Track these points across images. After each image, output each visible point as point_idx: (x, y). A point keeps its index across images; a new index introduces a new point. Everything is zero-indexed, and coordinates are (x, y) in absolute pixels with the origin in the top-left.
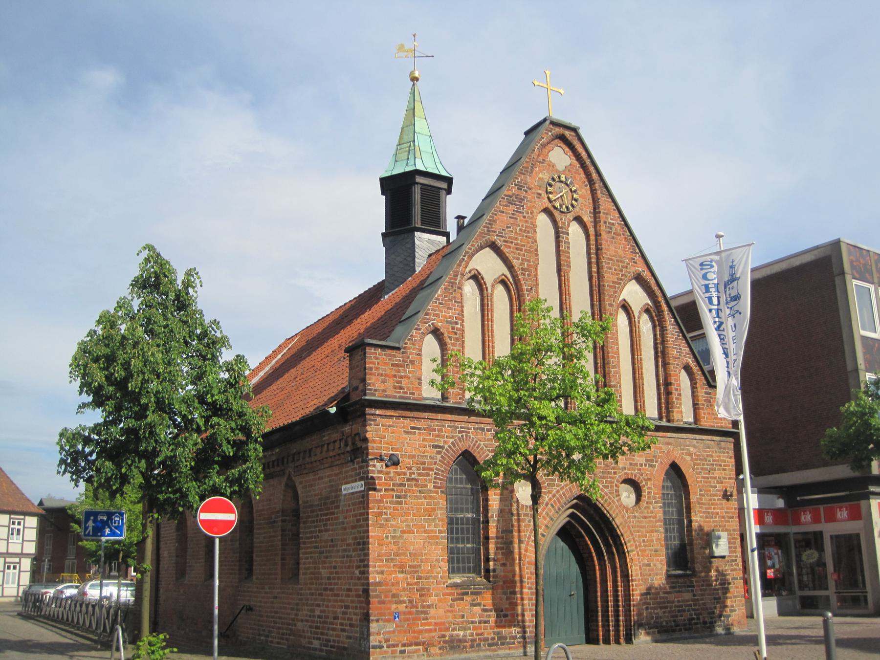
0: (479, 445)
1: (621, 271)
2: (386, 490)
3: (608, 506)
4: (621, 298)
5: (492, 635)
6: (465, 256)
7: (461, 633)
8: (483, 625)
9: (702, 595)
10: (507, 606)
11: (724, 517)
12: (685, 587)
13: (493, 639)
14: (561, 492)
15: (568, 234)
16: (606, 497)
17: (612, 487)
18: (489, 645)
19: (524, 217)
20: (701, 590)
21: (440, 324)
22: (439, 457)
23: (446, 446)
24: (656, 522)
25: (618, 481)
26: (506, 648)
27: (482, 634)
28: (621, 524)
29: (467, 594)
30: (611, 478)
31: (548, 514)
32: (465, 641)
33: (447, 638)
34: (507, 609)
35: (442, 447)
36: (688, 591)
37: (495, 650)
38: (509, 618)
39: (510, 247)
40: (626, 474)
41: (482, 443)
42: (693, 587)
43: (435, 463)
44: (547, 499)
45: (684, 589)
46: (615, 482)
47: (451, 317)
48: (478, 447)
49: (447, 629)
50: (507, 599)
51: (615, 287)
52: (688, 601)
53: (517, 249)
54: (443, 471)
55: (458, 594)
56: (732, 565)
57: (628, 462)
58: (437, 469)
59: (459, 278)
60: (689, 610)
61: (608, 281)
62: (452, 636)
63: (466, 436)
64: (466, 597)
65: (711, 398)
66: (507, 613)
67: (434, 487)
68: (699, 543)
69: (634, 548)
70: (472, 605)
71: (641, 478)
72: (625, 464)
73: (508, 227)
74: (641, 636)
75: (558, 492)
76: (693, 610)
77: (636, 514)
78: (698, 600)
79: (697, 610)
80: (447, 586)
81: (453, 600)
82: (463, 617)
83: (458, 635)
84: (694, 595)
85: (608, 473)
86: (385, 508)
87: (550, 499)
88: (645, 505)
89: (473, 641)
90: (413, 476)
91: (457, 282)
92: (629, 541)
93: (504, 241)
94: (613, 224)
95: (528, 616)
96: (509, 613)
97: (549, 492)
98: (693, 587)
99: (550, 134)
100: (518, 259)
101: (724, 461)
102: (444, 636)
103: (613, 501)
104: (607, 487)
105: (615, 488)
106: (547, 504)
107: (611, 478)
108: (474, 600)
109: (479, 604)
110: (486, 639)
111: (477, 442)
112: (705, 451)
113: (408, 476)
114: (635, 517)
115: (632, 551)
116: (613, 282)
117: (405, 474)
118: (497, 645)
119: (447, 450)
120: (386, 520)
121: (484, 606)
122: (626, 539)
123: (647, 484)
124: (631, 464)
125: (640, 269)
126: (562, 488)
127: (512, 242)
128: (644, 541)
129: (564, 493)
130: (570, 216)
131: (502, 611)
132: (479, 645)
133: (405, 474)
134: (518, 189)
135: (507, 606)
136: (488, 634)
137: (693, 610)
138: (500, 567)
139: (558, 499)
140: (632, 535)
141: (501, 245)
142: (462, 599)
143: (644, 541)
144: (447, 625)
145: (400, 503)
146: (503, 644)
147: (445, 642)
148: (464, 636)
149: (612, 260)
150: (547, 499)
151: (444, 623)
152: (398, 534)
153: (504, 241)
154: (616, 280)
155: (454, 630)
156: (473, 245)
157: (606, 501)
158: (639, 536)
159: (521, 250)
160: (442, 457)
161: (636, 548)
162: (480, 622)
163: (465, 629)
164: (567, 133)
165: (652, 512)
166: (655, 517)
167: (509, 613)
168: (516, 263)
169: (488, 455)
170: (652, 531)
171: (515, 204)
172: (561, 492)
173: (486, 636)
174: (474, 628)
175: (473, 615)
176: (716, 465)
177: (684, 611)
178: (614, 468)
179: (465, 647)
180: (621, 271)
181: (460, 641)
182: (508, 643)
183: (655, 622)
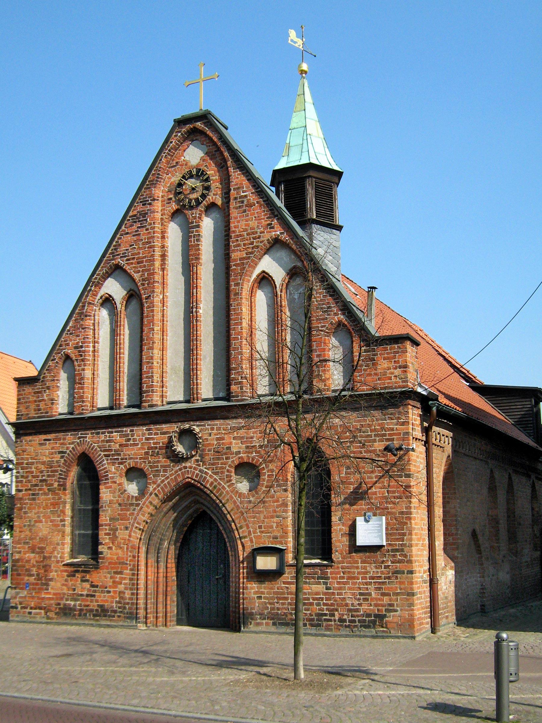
0: (94, 446)
1: (252, 243)
2: (26, 490)
3: (217, 492)
4: (257, 271)
5: (96, 608)
6: (91, 287)
7: (72, 603)
8: (89, 598)
9: (340, 589)
10: (111, 584)
11: (386, 498)
12: (313, 578)
13: (97, 610)
14: (166, 482)
15: (198, 226)
16: (215, 483)
17: (222, 473)
18: (95, 615)
19: (147, 230)
20: (339, 583)
21: (69, 351)
22: (62, 460)
23: (68, 451)
24: (278, 506)
25: (230, 466)
26: (107, 620)
27: (88, 606)
28: (232, 510)
29: (77, 571)
30: (222, 464)
31: (151, 503)
32: (75, 610)
33: (62, 606)
34: (110, 587)
35: (65, 453)
36: (319, 583)
37: (97, 620)
38: (112, 594)
39: (132, 263)
40: (242, 457)
41: (96, 445)
42: (328, 578)
43: (59, 466)
44: (151, 489)
45: (312, 580)
46: (227, 468)
47: (78, 343)
48: (92, 449)
49: (62, 599)
50: (111, 578)
51: (243, 264)
52: (318, 593)
53: (138, 263)
54: (65, 472)
55: (72, 572)
56: (394, 556)
57: (244, 445)
58: (61, 471)
59: (86, 308)
60: (318, 604)
61: (235, 260)
62: (65, 605)
63: (84, 440)
64: (77, 575)
65: (376, 355)
66: (110, 590)
67: (59, 485)
68: (340, 530)
69: (246, 534)
70: (83, 581)
71: (261, 460)
72: (240, 448)
73: (131, 246)
74: (251, 626)
75: (163, 481)
76: (324, 604)
77: (252, 499)
78: (333, 594)
79: (332, 605)
80: (64, 565)
81: (68, 576)
82: (74, 590)
83: (70, 605)
84: (327, 589)
85: (219, 459)
86: (25, 504)
87: (155, 489)
88: (264, 489)
89: (81, 610)
90: (44, 478)
91: (85, 311)
92: (241, 527)
93: (127, 260)
94: (246, 196)
95: (128, 594)
96: (112, 590)
97: (154, 483)
98: (328, 578)
99: (179, 134)
100: (139, 272)
101: (392, 429)
102: (59, 604)
103: (223, 487)
104: (216, 473)
105: (226, 473)
106: (151, 494)
107: (222, 464)
108: (84, 577)
109: (87, 581)
110: (91, 610)
111: (92, 444)
112: (359, 421)
113: (40, 478)
114: (250, 502)
115: (245, 537)
116: (241, 259)
117: (38, 477)
118: (99, 616)
119: (68, 454)
120: (25, 513)
121: (92, 582)
122: (238, 525)
123: (267, 466)
124: (247, 447)
125: (278, 233)
126: (168, 478)
127: (133, 259)
128: (260, 527)
129: (168, 483)
130: (201, 208)
131: (106, 588)
132: (85, 615)
133: (38, 477)
134: (143, 205)
135: (111, 584)
136: (94, 606)
137: (324, 604)
138: (106, 550)
139: (162, 488)
140: (245, 520)
141: (124, 265)
142: (74, 576)
143: (260, 527)
144: (62, 596)
145: (34, 499)
146: (105, 616)
147: (60, 608)
148: (75, 605)
149: (241, 236)
150: (151, 489)
151: (59, 594)
152: (32, 523)
153: (127, 260)
154: (245, 256)
155: (67, 600)
156: (98, 275)
157: (215, 487)
158: (254, 523)
159: (142, 262)
160: (65, 460)
161: (250, 532)
162: (87, 595)
163: (76, 600)
164: (199, 125)
165: (273, 497)
166: (277, 501)
167: (112, 590)
168: (136, 276)
169: (100, 455)
170: (272, 517)
171: (139, 221)
172: (166, 482)
173: (91, 607)
174: (83, 600)
175: (83, 589)
176: (375, 435)
177: (312, 604)
178: (226, 454)
179: (75, 615)
180: (252, 243)
181: (70, 609)
182: (110, 616)
183: (269, 613)
